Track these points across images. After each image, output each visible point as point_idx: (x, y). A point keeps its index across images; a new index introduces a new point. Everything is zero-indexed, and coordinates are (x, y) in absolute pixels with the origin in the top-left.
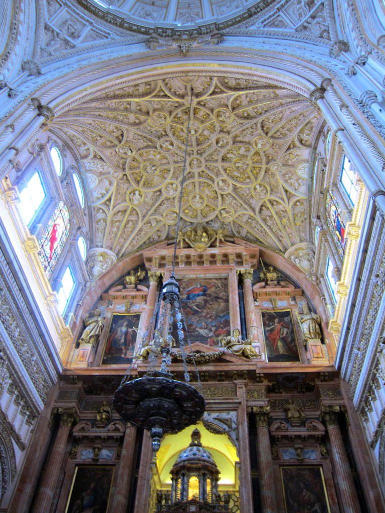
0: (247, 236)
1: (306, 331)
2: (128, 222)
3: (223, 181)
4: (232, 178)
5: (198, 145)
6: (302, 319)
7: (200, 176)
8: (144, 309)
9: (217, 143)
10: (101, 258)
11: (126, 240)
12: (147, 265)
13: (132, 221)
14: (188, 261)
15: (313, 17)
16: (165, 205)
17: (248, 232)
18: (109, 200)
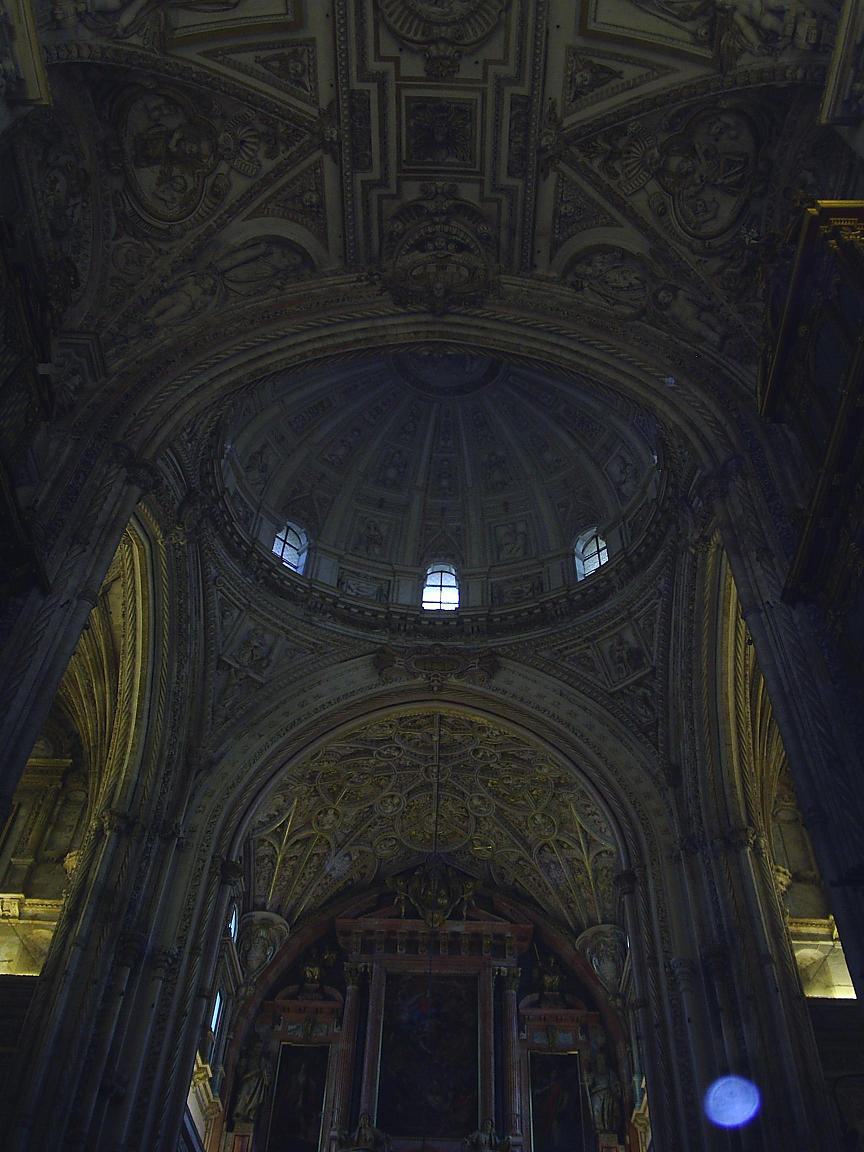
0: (514, 884)
1: (598, 1119)
2: (310, 859)
3: (481, 798)
4: (497, 795)
5: (441, 747)
6: (594, 1084)
7: (440, 785)
8: (340, 1048)
9: (476, 751)
10: (263, 933)
11: (306, 889)
12: (341, 940)
13: (318, 855)
14: (412, 944)
15: (638, 683)
16: (377, 828)
17: (516, 880)
18: (283, 826)
